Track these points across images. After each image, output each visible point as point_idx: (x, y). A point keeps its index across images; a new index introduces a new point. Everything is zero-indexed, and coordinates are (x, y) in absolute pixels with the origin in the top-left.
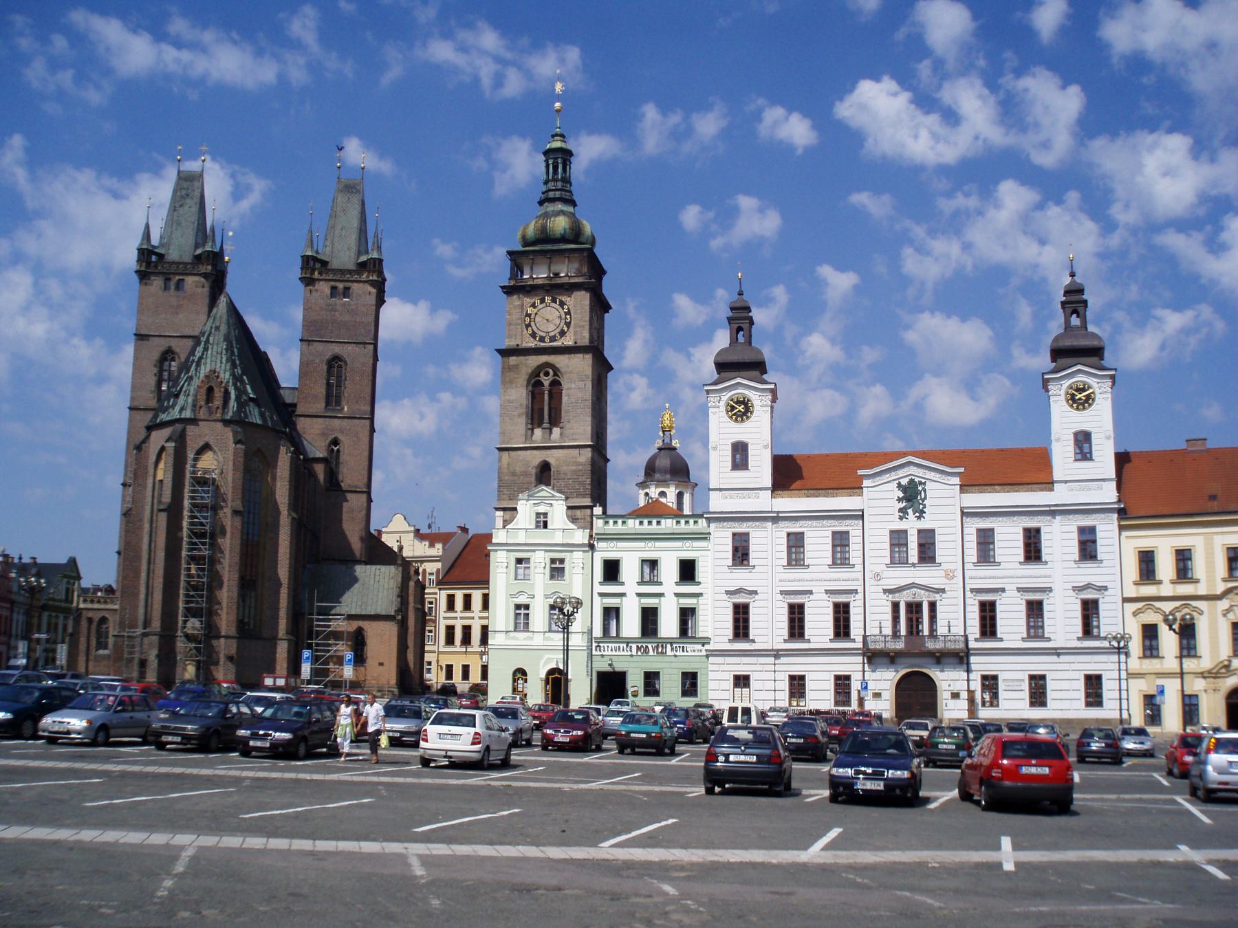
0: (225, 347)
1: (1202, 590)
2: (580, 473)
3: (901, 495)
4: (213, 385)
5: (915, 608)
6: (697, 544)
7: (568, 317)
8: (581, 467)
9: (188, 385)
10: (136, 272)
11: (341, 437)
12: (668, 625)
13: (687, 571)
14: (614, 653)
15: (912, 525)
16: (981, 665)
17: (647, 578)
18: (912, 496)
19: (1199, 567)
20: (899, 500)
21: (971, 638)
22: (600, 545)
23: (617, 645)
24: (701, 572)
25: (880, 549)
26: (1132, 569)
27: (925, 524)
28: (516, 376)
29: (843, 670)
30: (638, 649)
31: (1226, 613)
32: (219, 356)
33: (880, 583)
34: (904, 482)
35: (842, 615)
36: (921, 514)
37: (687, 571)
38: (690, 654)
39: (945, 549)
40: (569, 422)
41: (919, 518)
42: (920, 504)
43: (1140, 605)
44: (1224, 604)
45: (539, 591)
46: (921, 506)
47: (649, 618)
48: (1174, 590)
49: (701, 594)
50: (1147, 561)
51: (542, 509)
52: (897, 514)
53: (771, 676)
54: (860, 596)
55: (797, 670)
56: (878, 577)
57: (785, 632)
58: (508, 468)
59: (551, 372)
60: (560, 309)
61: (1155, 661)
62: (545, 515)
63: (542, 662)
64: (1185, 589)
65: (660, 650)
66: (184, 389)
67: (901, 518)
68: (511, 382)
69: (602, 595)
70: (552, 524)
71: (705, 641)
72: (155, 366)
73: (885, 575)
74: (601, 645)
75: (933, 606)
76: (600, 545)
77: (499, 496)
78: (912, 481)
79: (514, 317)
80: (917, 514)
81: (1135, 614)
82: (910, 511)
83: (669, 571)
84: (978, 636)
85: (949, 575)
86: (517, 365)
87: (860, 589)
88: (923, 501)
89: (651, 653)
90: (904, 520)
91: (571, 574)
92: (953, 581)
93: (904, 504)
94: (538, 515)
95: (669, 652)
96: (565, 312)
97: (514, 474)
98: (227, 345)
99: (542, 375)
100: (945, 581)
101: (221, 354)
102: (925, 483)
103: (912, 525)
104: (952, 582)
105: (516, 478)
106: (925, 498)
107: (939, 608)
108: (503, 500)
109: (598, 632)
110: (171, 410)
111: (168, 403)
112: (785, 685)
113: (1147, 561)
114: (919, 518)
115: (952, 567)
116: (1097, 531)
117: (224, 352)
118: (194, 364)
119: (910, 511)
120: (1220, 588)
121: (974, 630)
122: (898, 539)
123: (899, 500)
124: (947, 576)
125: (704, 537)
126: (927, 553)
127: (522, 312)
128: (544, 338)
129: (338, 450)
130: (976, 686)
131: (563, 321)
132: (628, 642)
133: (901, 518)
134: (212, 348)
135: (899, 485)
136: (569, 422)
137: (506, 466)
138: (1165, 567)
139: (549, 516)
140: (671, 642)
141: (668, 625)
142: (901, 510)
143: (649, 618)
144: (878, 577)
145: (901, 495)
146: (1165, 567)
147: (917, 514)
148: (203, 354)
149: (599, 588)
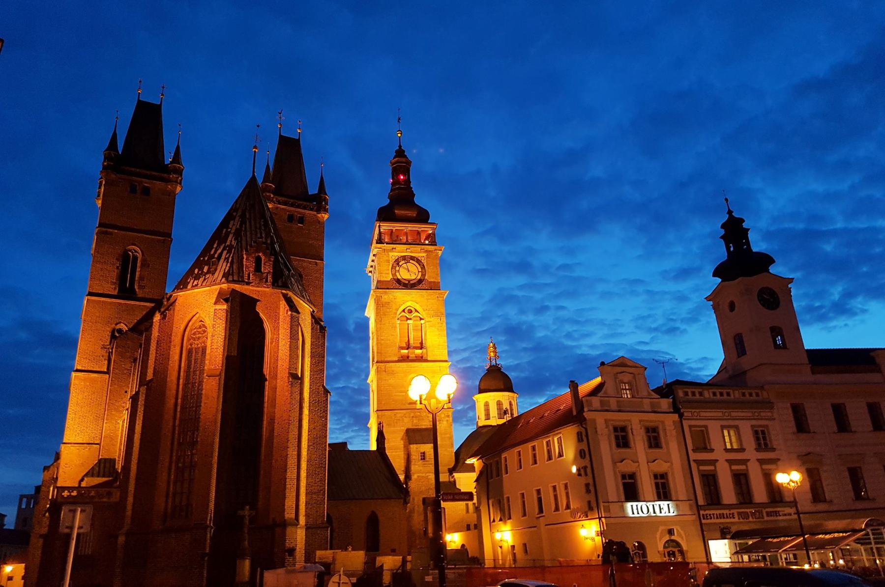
0: (262, 223)
4: (260, 254)
7: (423, 271)
9: (229, 252)
28: (388, 310)
32: (258, 231)
45: (642, 458)
66: (223, 257)
72: (117, 259)
86: (388, 303)
91: (667, 444)
96: (421, 267)
98: (263, 222)
99: (406, 311)
101: (260, 229)
110: (207, 276)
111: (201, 269)
117: (263, 228)
118: (231, 236)
128: (407, 284)
131: (420, 273)
132: (730, 507)
134: (250, 222)
148: (241, 226)
149: (693, 456)
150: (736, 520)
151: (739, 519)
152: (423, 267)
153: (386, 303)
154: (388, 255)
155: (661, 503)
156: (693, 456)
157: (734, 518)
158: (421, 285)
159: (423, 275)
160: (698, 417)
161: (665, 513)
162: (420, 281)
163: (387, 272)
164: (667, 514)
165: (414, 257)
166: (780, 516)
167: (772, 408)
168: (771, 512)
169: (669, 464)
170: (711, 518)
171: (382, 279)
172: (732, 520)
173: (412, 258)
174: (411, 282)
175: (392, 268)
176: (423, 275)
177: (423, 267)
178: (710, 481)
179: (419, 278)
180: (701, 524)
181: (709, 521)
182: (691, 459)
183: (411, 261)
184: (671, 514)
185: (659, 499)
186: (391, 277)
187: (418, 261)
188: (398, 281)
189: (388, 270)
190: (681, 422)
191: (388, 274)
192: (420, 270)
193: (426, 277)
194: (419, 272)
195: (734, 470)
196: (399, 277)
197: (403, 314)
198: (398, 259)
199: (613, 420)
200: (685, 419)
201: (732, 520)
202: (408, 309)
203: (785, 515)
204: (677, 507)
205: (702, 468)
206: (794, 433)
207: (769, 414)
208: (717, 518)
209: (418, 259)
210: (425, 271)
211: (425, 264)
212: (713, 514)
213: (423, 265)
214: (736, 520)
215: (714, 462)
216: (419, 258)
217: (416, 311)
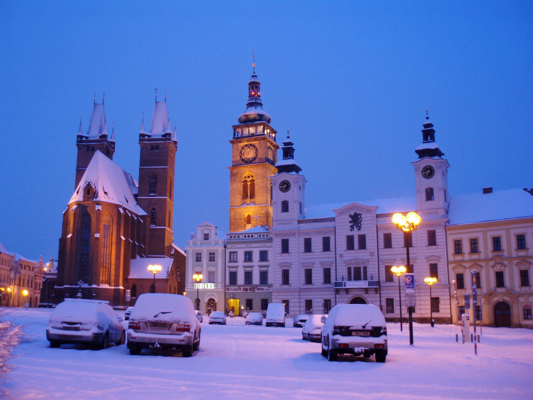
1: (482, 256)
2: (262, 218)
3: (351, 220)
5: (357, 270)
6: (269, 244)
8: (262, 215)
10: (76, 144)
11: (155, 207)
12: (256, 279)
13: (264, 256)
14: (234, 291)
15: (356, 233)
16: (386, 294)
17: (247, 260)
18: (356, 220)
19: (481, 246)
20: (350, 222)
21: (381, 282)
22: (229, 246)
23: (235, 288)
24: (270, 256)
25: (342, 243)
26: (451, 249)
27: (361, 232)
28: (236, 178)
29: (327, 297)
30: (244, 289)
31: (493, 267)
33: (344, 258)
34: (352, 214)
35: (327, 273)
36: (359, 228)
37: (264, 256)
38: (264, 291)
39: (370, 243)
40: (257, 196)
41: (359, 230)
42: (359, 224)
43: (455, 265)
44: (492, 263)
46: (360, 225)
47: (248, 276)
48: (470, 257)
49: (269, 266)
50: (458, 245)
51: (206, 232)
52: (349, 228)
53: (298, 300)
54: (334, 265)
55: (309, 298)
56: (341, 256)
57: (303, 281)
58: (233, 217)
59: (251, 176)
60: (254, 149)
61: (462, 291)
62: (208, 235)
63: (206, 296)
64: (475, 257)
65: (252, 289)
67: (351, 230)
68: (234, 181)
69: (230, 267)
70: (210, 238)
71: (271, 286)
73: (345, 255)
74: (229, 288)
75: (365, 268)
76: (229, 246)
77: (230, 228)
78: (355, 213)
79: (235, 153)
80: (358, 228)
81: (453, 269)
82: (355, 227)
83: (256, 256)
84: (385, 281)
85: (372, 254)
87: (334, 262)
88: (360, 222)
89: (249, 291)
90: (353, 231)
92: (374, 257)
93: (352, 224)
94: (205, 235)
95: (256, 291)
97: (236, 219)
100: (370, 257)
102: (361, 214)
103: (356, 233)
104: (373, 257)
105: (237, 221)
106: (361, 221)
107: (368, 270)
108: (232, 230)
109: (228, 282)
112: (303, 304)
113: (458, 245)
114: (359, 230)
115: (373, 251)
116: (436, 232)
119: (355, 227)
120: (490, 255)
121: (383, 278)
122: (350, 240)
123: (350, 222)
124: (371, 255)
125: (270, 240)
126: (363, 245)
127: (238, 151)
129: (155, 212)
130: (384, 303)
131: (255, 154)
132: (241, 286)
133: (351, 230)
135: (350, 216)
136: (257, 196)
137: (232, 216)
138: (466, 247)
139: (209, 235)
140: (257, 286)
141: (256, 279)
142: (351, 227)
143: (248, 276)
144: (341, 256)
145: (351, 220)
146: (466, 247)
147: (358, 228)
149: (228, 264)
150: (242, 291)
151: (243, 291)
152: (257, 150)
153: (235, 174)
154: (238, 145)
155: (208, 284)
156: (228, 264)
157: (241, 290)
158: (255, 161)
159: (257, 155)
160: (234, 248)
161: (209, 288)
162: (255, 159)
163: (237, 155)
164: (210, 288)
165: (252, 144)
166: (264, 290)
167: (271, 242)
168: (259, 289)
169: (216, 268)
170: (230, 290)
171: (235, 160)
172: (240, 291)
173: (251, 145)
174: (250, 160)
175: (240, 153)
176: (257, 155)
177: (257, 150)
178: (233, 276)
179: (254, 157)
180: (225, 293)
181: (229, 291)
182: (227, 265)
183: (250, 147)
184: (212, 288)
185: (209, 282)
186: (239, 158)
187: (254, 146)
188: (243, 160)
189: (237, 154)
190: (225, 250)
191: (237, 156)
192: (255, 152)
193: (258, 156)
194: (254, 153)
195: (261, 270)
196: (243, 158)
197: (245, 179)
198: (243, 147)
199: (195, 250)
200: (227, 249)
201: (240, 291)
202: (249, 175)
203: (266, 290)
204: (216, 286)
205: (231, 269)
206: (280, 253)
207: (271, 245)
208: (233, 290)
209: (254, 145)
210: (258, 152)
211: (258, 148)
212: (232, 289)
213: (257, 149)
214: (242, 291)
215: (252, 267)
216: (255, 145)
217: (252, 177)
